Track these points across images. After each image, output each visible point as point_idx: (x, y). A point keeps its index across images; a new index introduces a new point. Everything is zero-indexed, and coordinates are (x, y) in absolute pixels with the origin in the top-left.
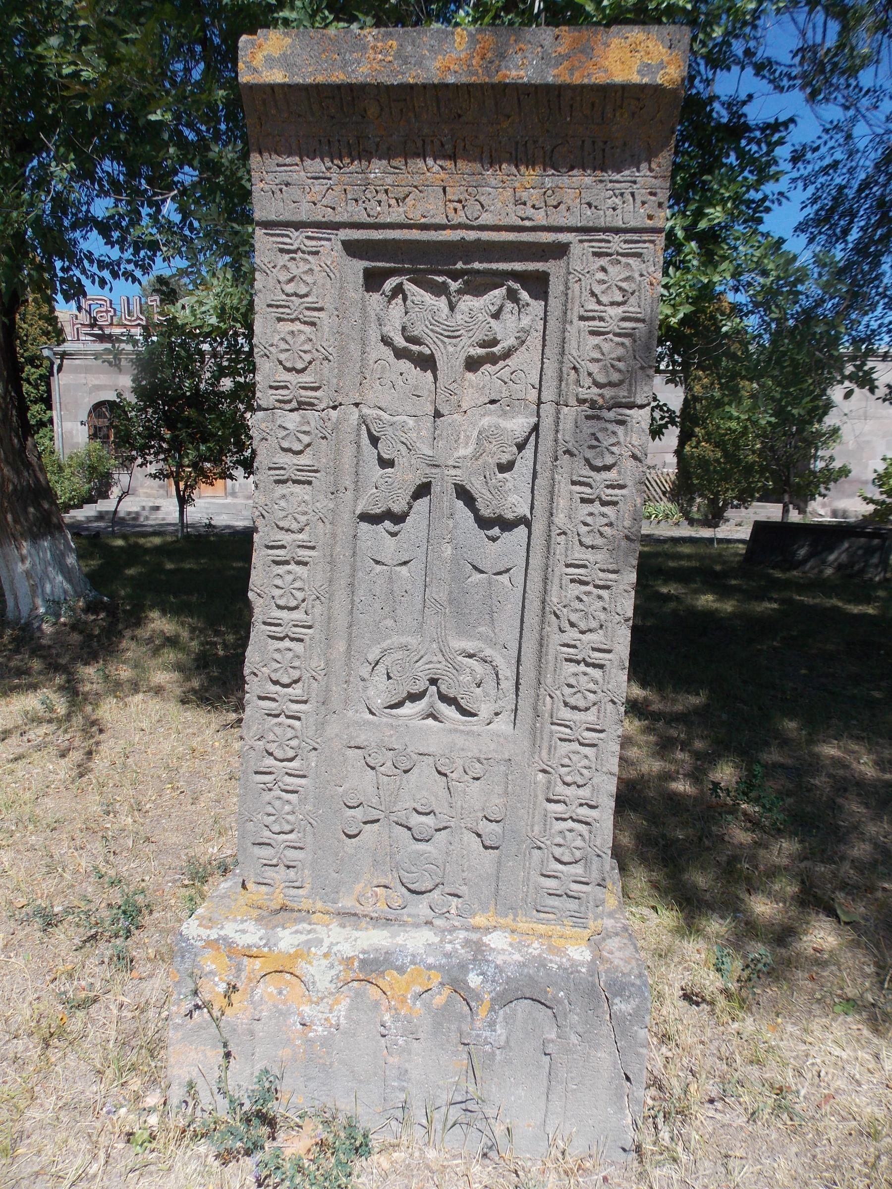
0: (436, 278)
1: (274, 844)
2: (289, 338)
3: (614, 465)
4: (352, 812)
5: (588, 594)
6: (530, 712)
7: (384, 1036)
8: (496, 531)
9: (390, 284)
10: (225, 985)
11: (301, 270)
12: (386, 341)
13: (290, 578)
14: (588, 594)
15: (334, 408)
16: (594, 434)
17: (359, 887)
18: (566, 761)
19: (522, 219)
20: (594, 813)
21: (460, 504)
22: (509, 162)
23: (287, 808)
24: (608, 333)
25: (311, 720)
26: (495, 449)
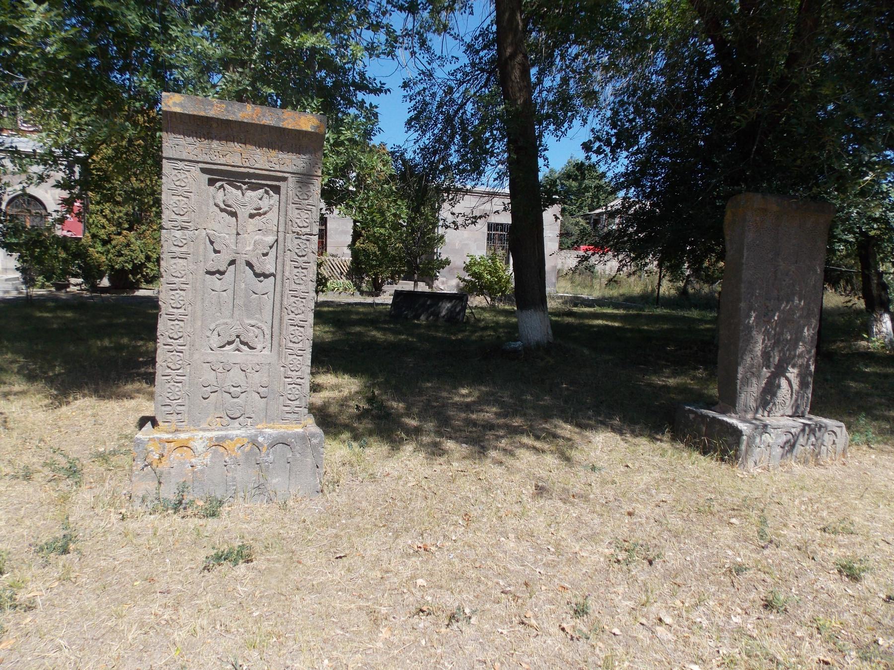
2: (177, 202)
5: (298, 301)
6: (277, 345)
7: (226, 466)
8: (262, 278)
9: (218, 184)
12: (216, 205)
13: (177, 296)
14: (298, 301)
17: (209, 419)
18: (292, 362)
23: (177, 389)
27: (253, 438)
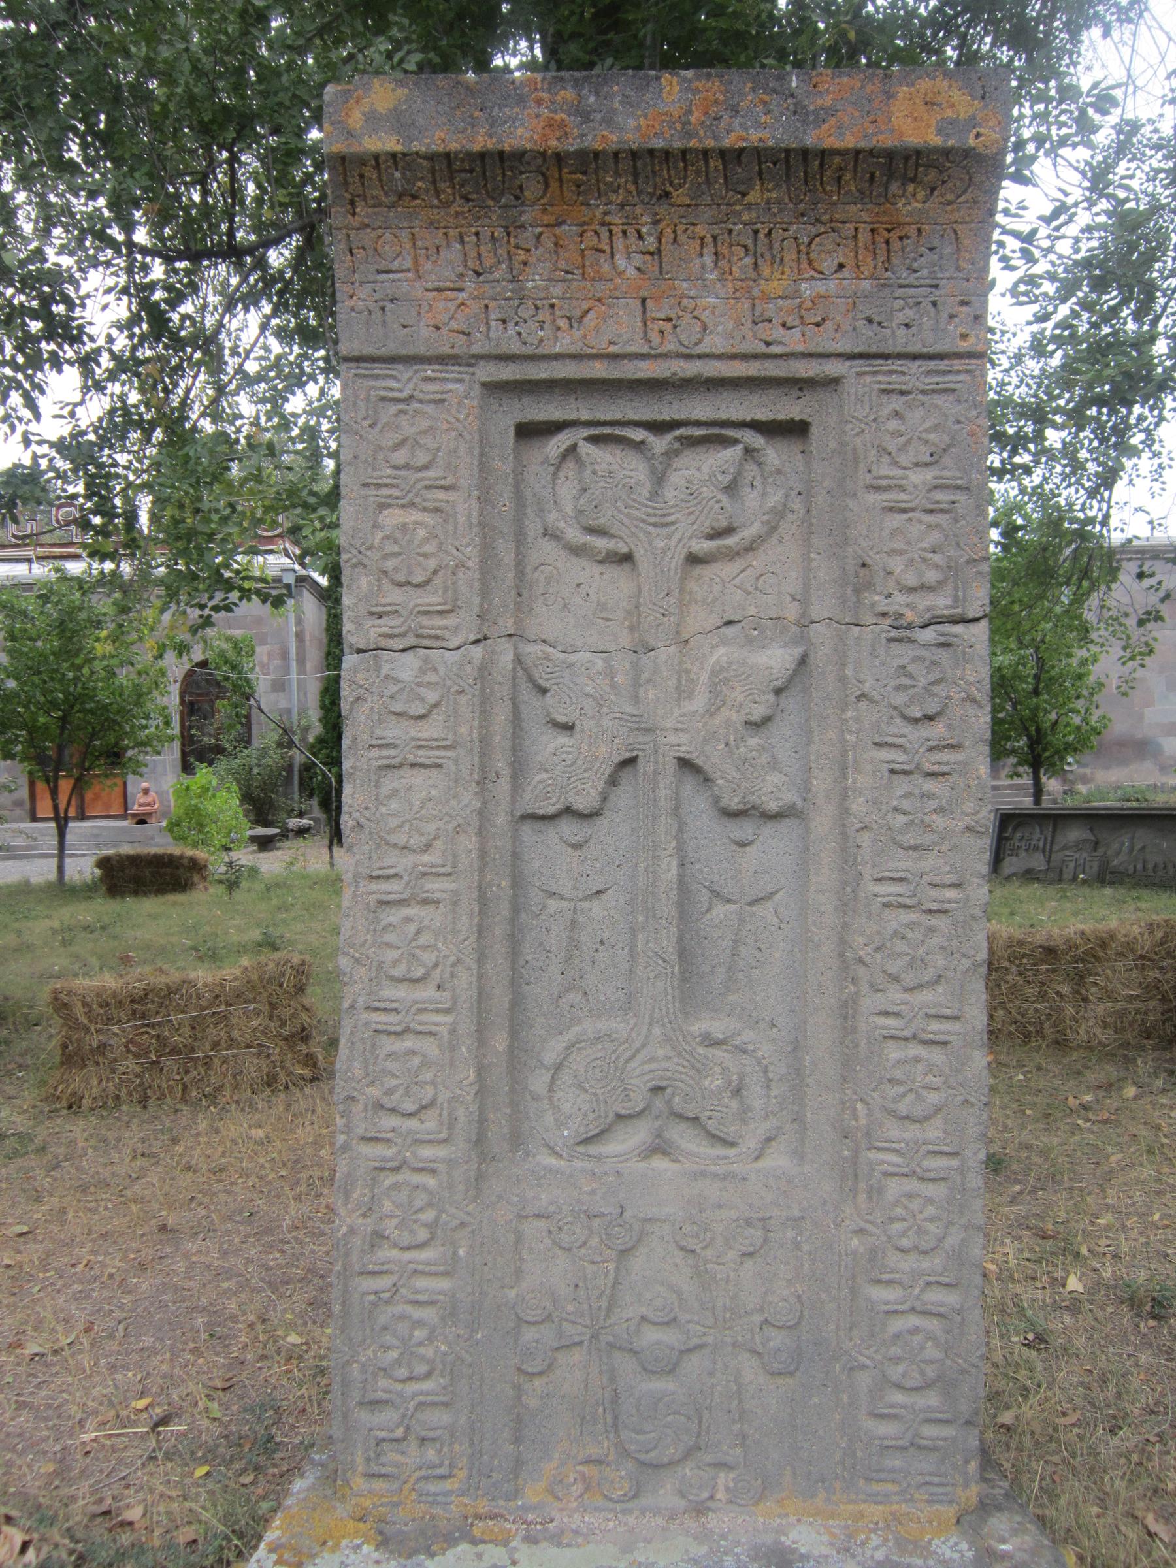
2: (398, 535)
3: (938, 714)
19: (768, 344)
26: (741, 698)
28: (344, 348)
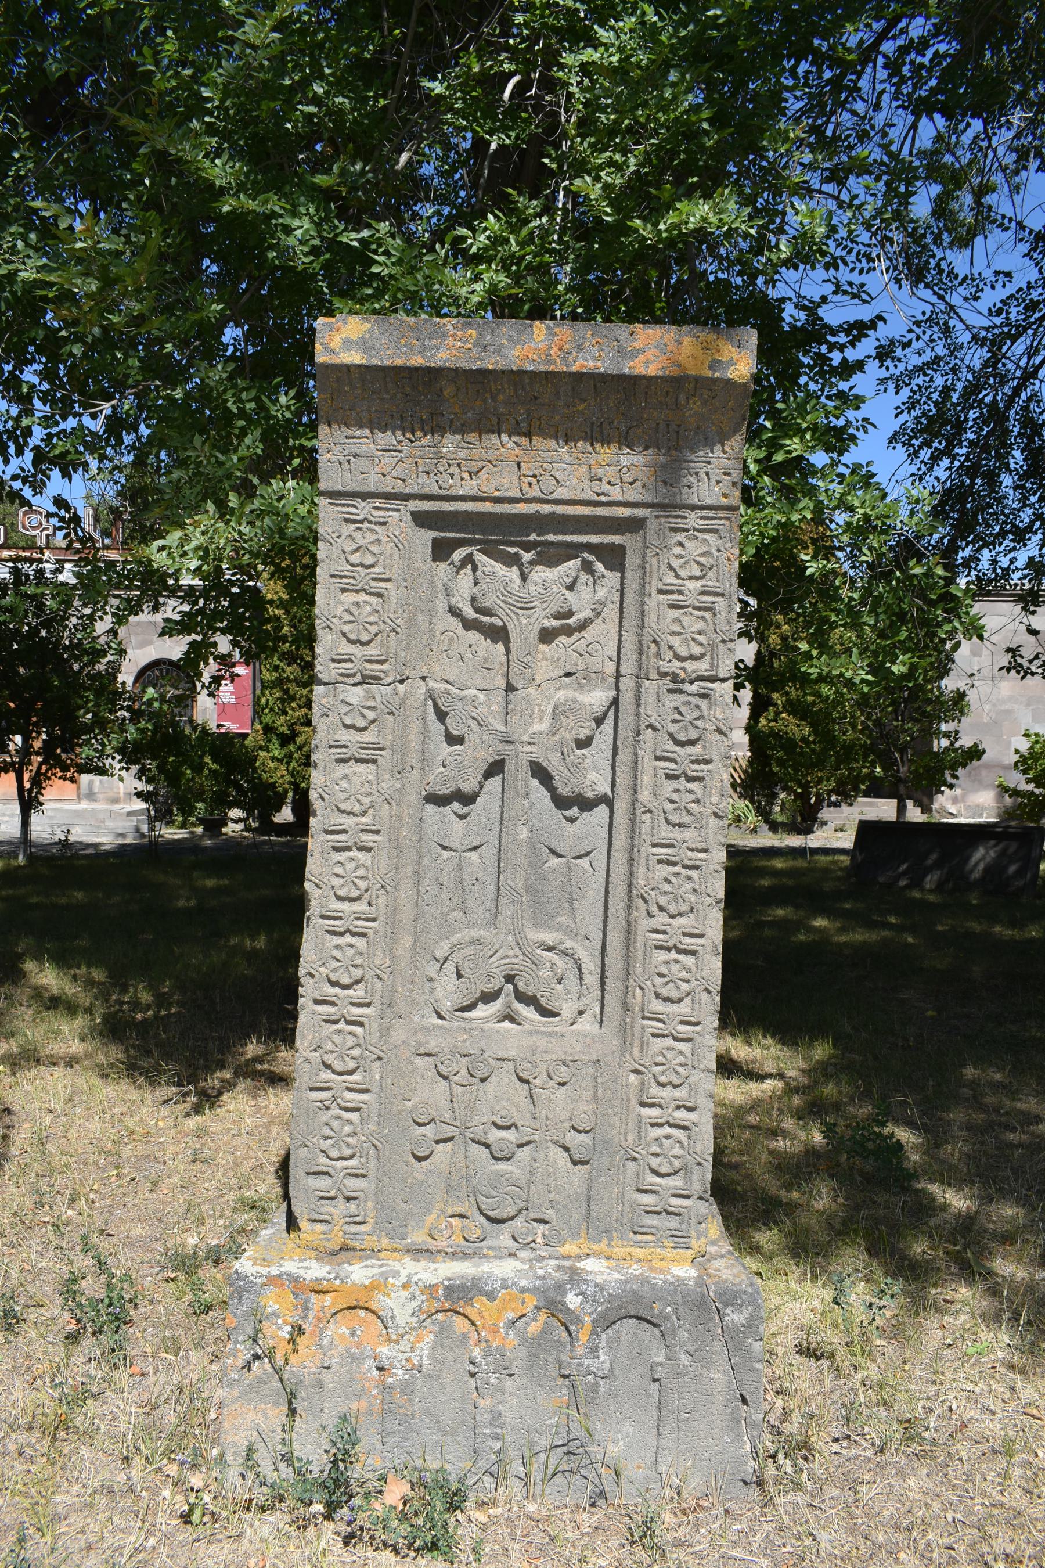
0: (508, 549)
1: (332, 1172)
2: (353, 609)
3: (698, 740)
4: (421, 1130)
7: (473, 1375)
8: (574, 811)
9: (458, 555)
10: (289, 1328)
11: (367, 540)
12: (454, 612)
13: (350, 866)
14: (676, 875)
15: (402, 682)
16: (676, 708)
17: (430, 1219)
19: (598, 495)
20: (692, 1116)
21: (535, 782)
22: (585, 440)
23: (348, 1129)
24: (687, 607)
25: (375, 1025)
26: (572, 724)
27: (552, 1294)
28: (322, 485)
